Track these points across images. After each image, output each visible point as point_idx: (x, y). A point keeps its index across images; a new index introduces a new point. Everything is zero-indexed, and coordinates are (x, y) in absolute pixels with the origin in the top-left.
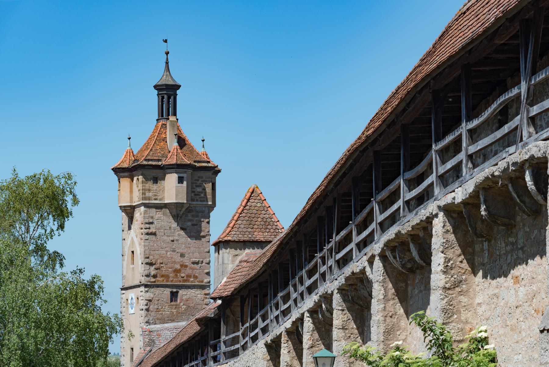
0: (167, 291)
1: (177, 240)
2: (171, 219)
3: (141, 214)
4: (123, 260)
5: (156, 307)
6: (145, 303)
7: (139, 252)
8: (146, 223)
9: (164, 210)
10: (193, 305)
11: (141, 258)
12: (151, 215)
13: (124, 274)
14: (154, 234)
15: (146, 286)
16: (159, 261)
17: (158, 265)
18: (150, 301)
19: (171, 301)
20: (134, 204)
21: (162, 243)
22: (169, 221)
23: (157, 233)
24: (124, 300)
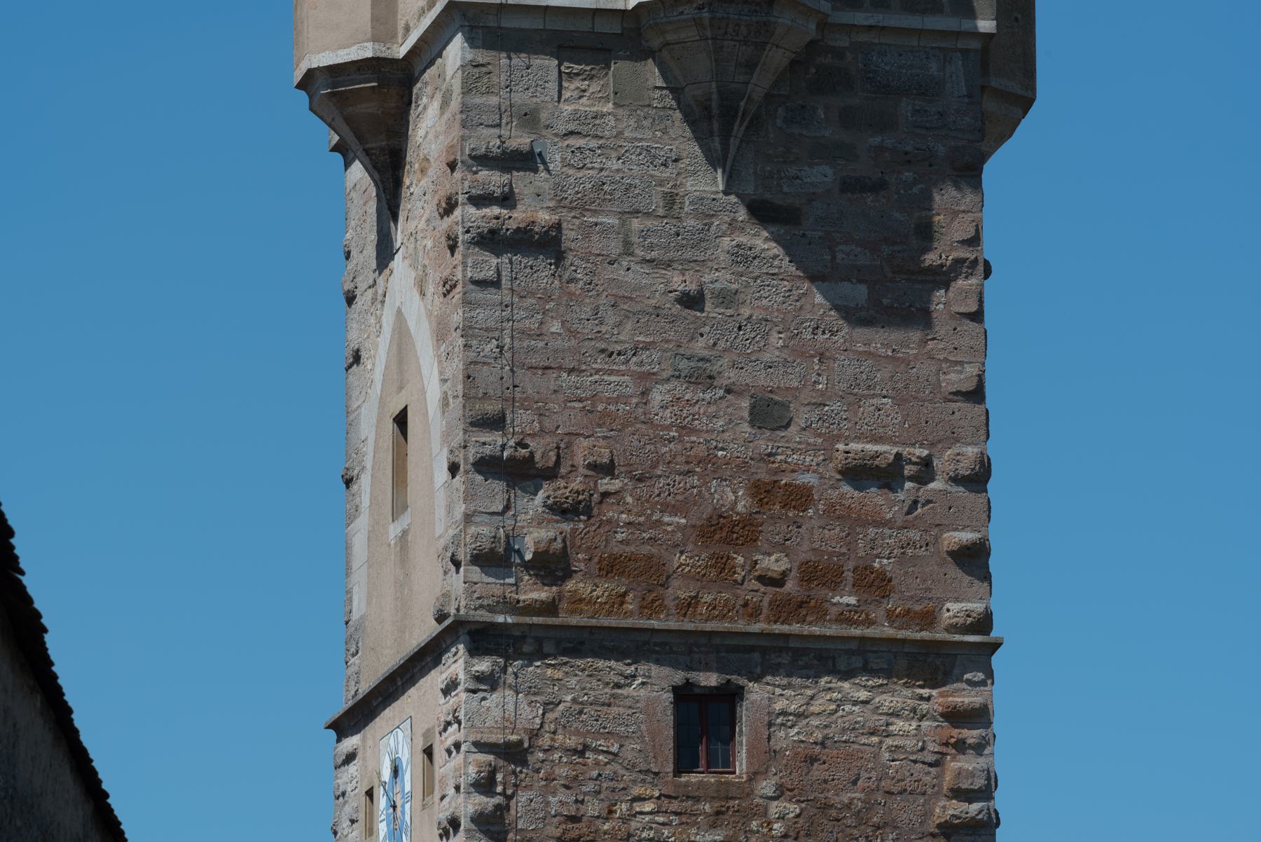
0: (651, 689)
1: (727, 298)
2: (679, 139)
3: (445, 104)
4: (350, 518)
5: (560, 800)
6: (472, 770)
7: (434, 392)
8: (484, 160)
9: (620, 67)
10: (855, 795)
11: (447, 435)
12: (518, 98)
13: (355, 616)
14: (544, 244)
15: (482, 638)
16: (581, 452)
17: (577, 483)
18: (513, 753)
19: (685, 763)
20: (402, 51)
21: (611, 318)
22: (667, 148)
23: (569, 234)
24: (356, 800)
